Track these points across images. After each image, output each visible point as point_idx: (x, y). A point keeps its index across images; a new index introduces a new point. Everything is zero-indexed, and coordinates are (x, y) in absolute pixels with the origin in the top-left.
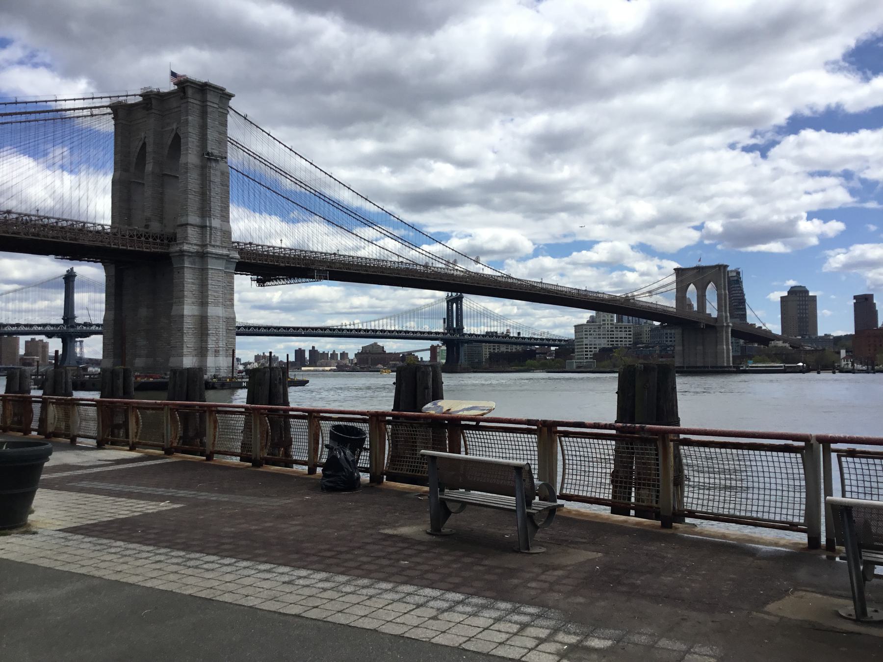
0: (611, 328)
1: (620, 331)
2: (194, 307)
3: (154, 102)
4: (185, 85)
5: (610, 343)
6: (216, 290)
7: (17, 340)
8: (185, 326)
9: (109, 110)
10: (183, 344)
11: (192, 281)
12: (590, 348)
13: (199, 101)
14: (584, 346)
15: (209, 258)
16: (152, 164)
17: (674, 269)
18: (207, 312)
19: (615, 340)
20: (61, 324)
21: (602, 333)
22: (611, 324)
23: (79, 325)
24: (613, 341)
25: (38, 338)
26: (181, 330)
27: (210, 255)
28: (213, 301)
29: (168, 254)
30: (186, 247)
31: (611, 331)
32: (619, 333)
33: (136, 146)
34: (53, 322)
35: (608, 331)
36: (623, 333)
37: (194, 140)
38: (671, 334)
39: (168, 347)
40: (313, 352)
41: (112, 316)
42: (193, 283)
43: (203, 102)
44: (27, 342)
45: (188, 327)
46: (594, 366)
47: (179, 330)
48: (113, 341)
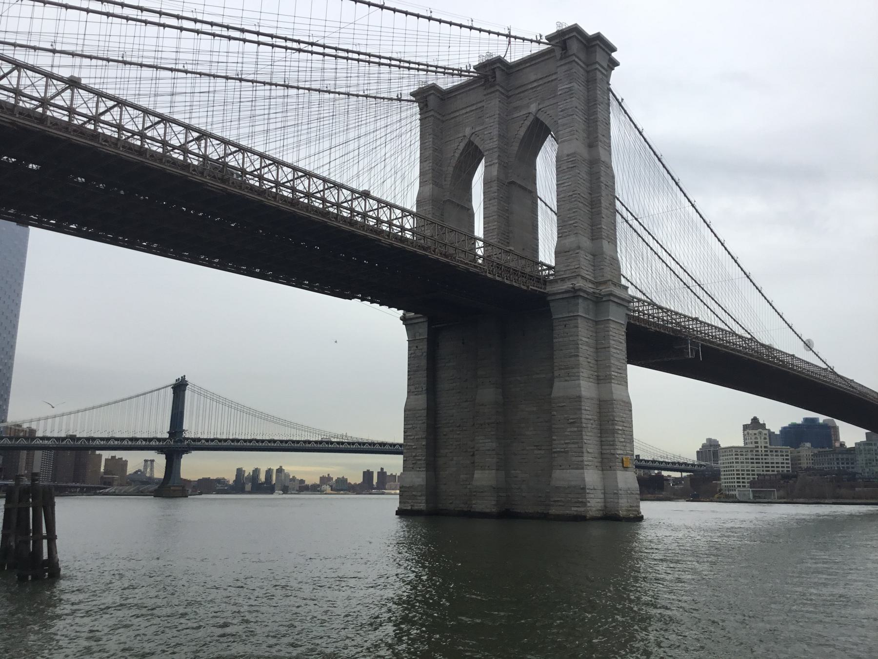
0: (765, 451)
1: (776, 456)
2: (590, 384)
3: (498, 73)
4: (567, 37)
5: (765, 469)
6: (618, 356)
7: (100, 456)
8: (584, 416)
9: (412, 98)
10: (582, 447)
11: (587, 340)
12: (743, 474)
13: (584, 63)
14: (735, 472)
15: (611, 303)
16: (497, 165)
18: (612, 393)
19: (770, 465)
21: (755, 457)
22: (765, 447)
23: (187, 439)
24: (768, 467)
25: (118, 454)
26: (576, 422)
27: (612, 298)
28: (616, 374)
29: (547, 294)
30: (580, 283)
31: (765, 455)
32: (775, 457)
33: (455, 149)
34: (159, 436)
35: (762, 455)
36: (780, 457)
37: (581, 120)
38: (842, 459)
39: (536, 452)
40: (382, 474)
41: (422, 401)
42: (587, 344)
43: (587, 66)
44: (106, 460)
45: (588, 417)
46: (774, 495)
47: (572, 423)
48: (424, 443)
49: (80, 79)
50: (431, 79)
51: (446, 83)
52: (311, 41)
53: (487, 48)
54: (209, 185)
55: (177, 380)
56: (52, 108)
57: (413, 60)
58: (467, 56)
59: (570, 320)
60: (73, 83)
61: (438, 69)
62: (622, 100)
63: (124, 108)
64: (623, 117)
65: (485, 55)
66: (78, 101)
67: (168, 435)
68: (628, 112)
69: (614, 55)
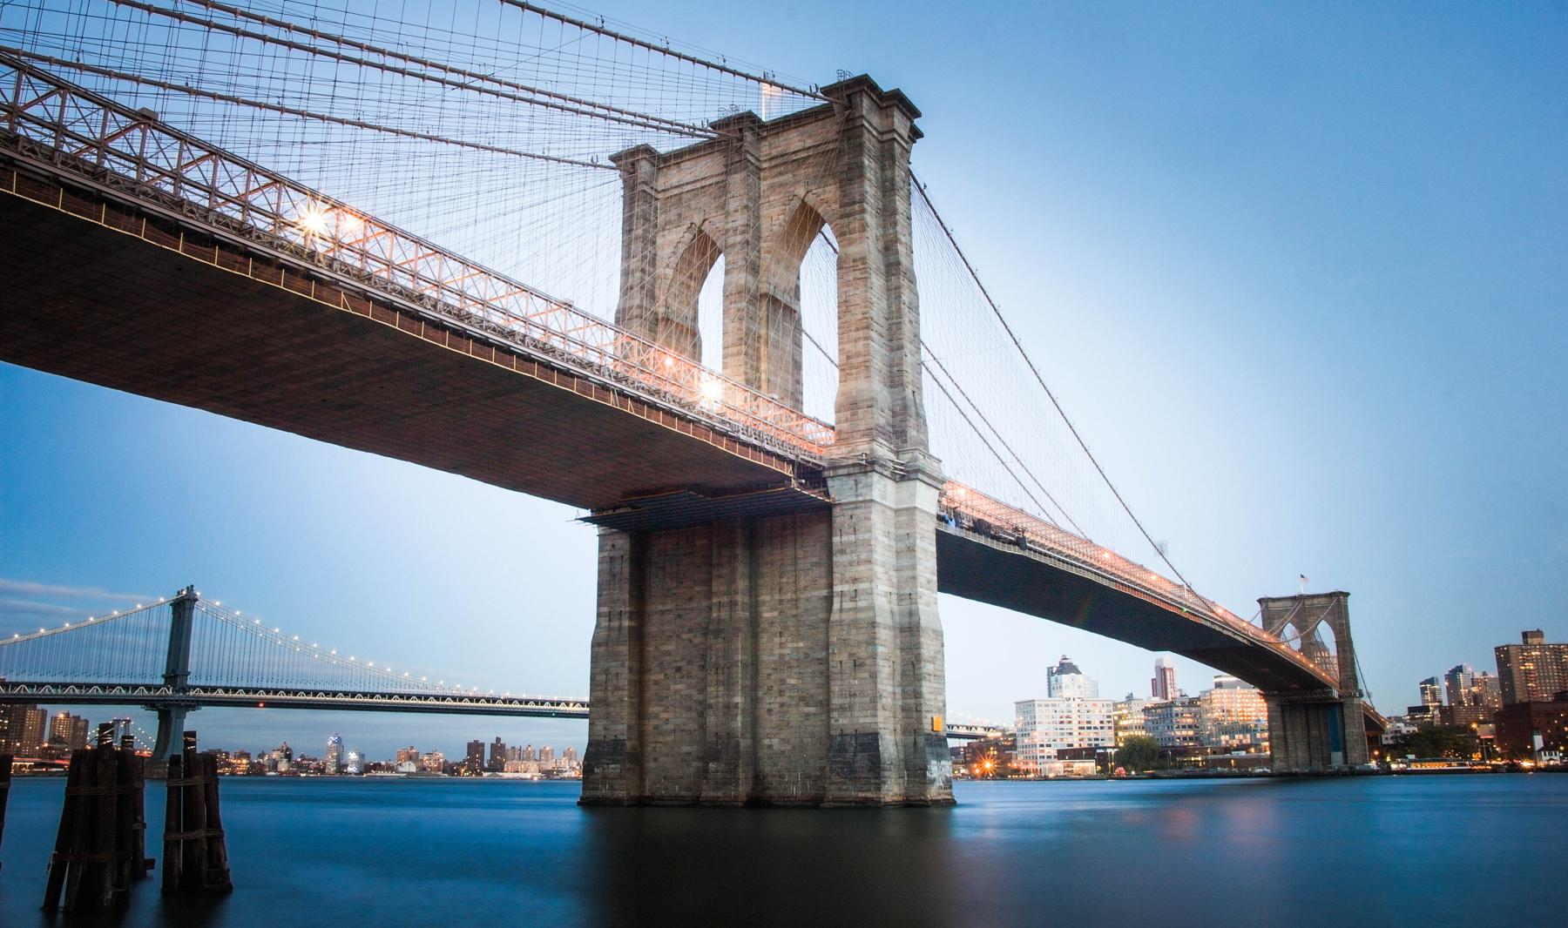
9: (613, 164)
17: (1260, 601)
20: (164, 686)
27: (920, 476)
49: (156, 114)
50: (640, 137)
51: (665, 144)
52: (482, 73)
53: (731, 99)
54: (340, 283)
55: (179, 593)
56: (110, 157)
57: (625, 108)
58: (703, 108)
59: (857, 508)
60: (146, 120)
61: (659, 125)
62: (925, 186)
63: (219, 162)
64: (927, 213)
65: (727, 108)
66: (151, 148)
67: (163, 680)
68: (932, 203)
69: (917, 122)
